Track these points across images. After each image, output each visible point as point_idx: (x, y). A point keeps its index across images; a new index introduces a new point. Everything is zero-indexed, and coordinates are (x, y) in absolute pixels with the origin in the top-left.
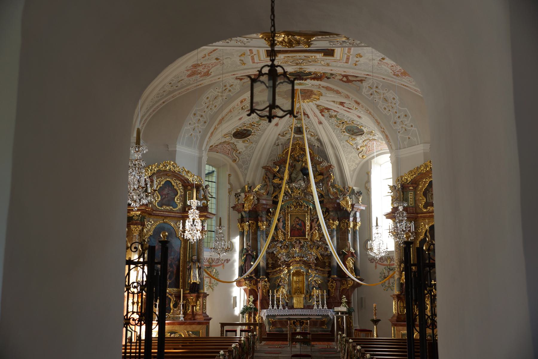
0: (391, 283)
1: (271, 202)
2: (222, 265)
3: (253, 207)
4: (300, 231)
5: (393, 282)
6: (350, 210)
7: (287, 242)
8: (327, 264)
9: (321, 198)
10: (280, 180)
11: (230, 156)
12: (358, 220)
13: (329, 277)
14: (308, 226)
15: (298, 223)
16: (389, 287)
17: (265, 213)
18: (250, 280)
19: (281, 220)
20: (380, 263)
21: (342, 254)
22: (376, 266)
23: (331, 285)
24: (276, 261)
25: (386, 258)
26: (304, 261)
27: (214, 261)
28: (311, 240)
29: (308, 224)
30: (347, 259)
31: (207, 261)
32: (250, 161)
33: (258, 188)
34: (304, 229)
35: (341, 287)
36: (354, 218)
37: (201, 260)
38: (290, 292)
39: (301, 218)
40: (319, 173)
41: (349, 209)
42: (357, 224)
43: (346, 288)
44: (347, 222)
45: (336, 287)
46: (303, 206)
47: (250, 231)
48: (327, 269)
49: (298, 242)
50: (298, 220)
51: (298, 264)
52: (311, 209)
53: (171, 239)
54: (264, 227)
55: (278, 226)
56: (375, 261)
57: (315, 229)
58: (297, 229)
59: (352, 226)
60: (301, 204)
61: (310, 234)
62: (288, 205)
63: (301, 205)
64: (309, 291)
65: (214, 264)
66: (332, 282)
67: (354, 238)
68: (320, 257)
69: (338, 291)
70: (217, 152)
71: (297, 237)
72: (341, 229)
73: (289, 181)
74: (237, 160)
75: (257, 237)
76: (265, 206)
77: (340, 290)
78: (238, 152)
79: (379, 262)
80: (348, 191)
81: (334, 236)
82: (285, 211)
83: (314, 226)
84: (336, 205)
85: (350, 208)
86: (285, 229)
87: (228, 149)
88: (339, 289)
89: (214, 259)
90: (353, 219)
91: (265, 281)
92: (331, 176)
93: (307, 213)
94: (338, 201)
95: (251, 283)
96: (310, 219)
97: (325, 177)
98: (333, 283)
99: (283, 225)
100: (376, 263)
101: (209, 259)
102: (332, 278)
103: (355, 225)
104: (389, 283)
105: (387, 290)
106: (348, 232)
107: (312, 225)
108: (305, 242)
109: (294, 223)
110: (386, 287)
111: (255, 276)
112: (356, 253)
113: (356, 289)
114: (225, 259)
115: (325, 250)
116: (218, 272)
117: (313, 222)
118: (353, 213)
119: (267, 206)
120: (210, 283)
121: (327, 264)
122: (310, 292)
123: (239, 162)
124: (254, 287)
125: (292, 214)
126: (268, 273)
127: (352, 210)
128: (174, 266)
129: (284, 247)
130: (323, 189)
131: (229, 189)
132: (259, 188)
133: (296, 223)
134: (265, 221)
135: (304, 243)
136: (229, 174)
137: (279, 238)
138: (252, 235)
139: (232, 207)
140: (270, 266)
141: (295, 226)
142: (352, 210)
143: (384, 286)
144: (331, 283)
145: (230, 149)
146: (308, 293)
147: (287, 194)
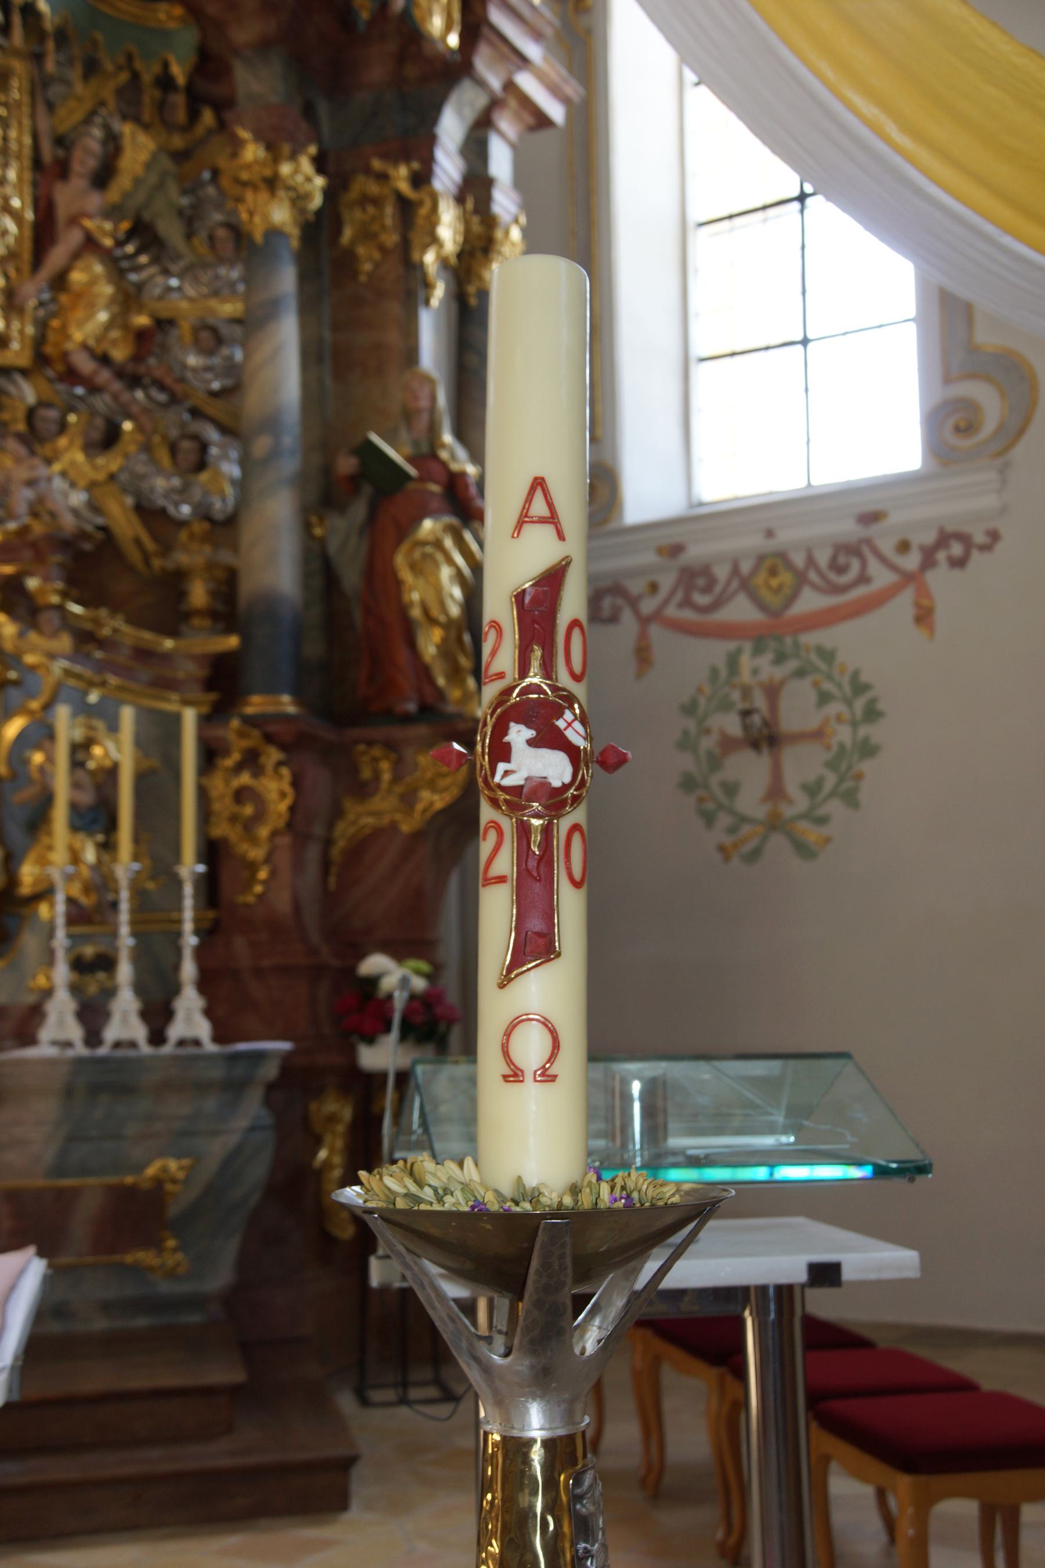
0: (792, 785)
5: (811, 778)
8: (198, 594)
16: (775, 824)
20: (688, 615)
21: (354, 482)
22: (643, 655)
23: (240, 795)
25: (746, 567)
28: (41, 359)
30: (406, 527)
35: (337, 813)
42: (499, 234)
43: (394, 826)
56: (633, 603)
69: (313, 854)
77: (328, 842)
79: (672, 611)
88: (318, 830)
98: (258, 771)
100: (644, 621)
104: (776, 792)
105: (754, 855)
110: (745, 829)
121: (198, 594)
143: (724, 820)
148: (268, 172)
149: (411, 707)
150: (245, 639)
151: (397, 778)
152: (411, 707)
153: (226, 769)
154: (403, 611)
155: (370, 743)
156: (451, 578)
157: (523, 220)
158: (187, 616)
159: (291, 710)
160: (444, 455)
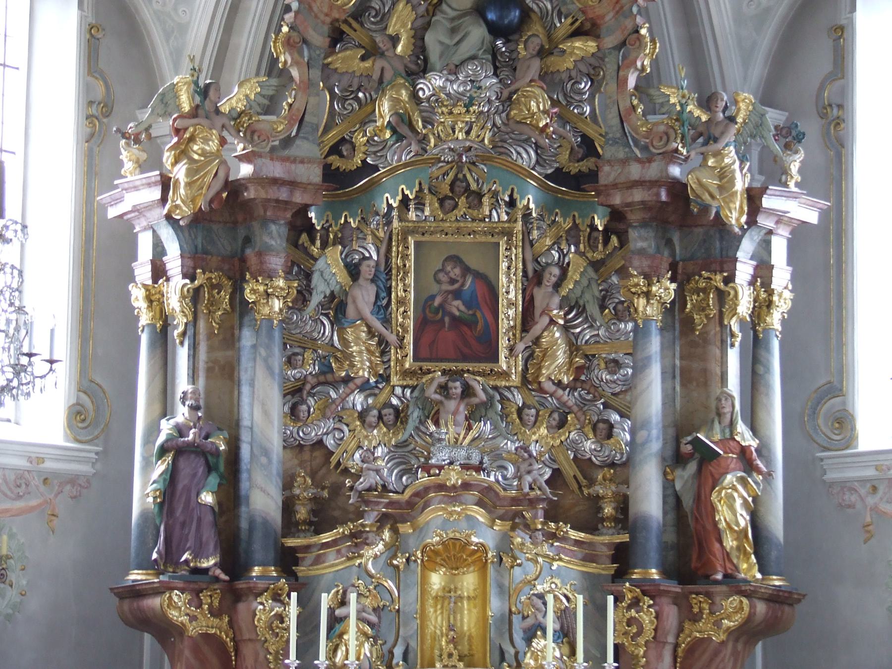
1: (315, 174)
3: (219, 193)
4: (465, 329)
6: (738, 220)
7: (398, 391)
8: (608, 510)
9: (582, 159)
10: (363, 58)
12: (781, 277)
13: (620, 575)
14: (511, 304)
15: (456, 286)
17: (284, 231)
18: (192, 586)
19: (367, 270)
24: (337, 490)
26: (488, 490)
29: (512, 295)
30: (716, 482)
33: (247, 96)
34: (490, 318)
36: (756, 268)
38: (411, 656)
39: (473, 262)
40: (577, 24)
41: (735, 216)
42: (775, 298)
43: (709, 639)
44: (721, 285)
45: (655, 630)
46: (486, 200)
47: (202, 324)
48: (608, 538)
49: (457, 387)
50: (457, 271)
51: (454, 500)
52: (527, 216)
54: (277, 304)
55: (350, 301)
57: (545, 320)
58: (454, 318)
59: (744, 307)
60: (474, 186)
61: (521, 346)
62: (407, 192)
63: (474, 192)
64: (512, 651)
66: (635, 603)
67: (754, 373)
68: (570, 471)
71: (449, 360)
72: (688, 324)
73: (413, 67)
75: (239, 360)
76: (283, 194)
77: (676, 646)
80: (732, 119)
81: (648, 360)
82: (389, 223)
83: (544, 306)
84: (668, 195)
85: (741, 212)
86: (387, 321)
88: (671, 639)
90: (751, 271)
91: (277, 598)
92: (640, 38)
93: (509, 234)
94: (675, 171)
95: (199, 606)
96: (525, 271)
97: (610, 41)
99: (377, 296)
102: (634, 583)
103: (762, 306)
106: (723, 342)
107: (532, 298)
108: (495, 388)
109: (434, 288)
111: (221, 565)
112: (764, 450)
113: (760, 645)
115: (598, 433)
117: (539, 283)
118: (752, 239)
119: (291, 192)
121: (608, 510)
122: (517, 653)
124: (216, 626)
125: (427, 238)
126: (294, 550)
127: (752, 222)
129: (380, 417)
130: (593, 110)
132: (252, 97)
133: (446, 287)
134: (281, 273)
135: (491, 398)
137: (352, 365)
138: (211, 349)
140: (302, 513)
141: (441, 306)
142: (752, 222)
144: (629, 607)
146: (503, 658)
147: (404, 130)
148: (645, 289)
149: (719, 577)
150: (632, 537)
151: (712, 613)
152: (719, 577)
153: (623, 607)
154: (715, 524)
155: (697, 594)
156: (742, 504)
157: (790, 287)
158: (603, 520)
159: (656, 577)
160: (738, 438)
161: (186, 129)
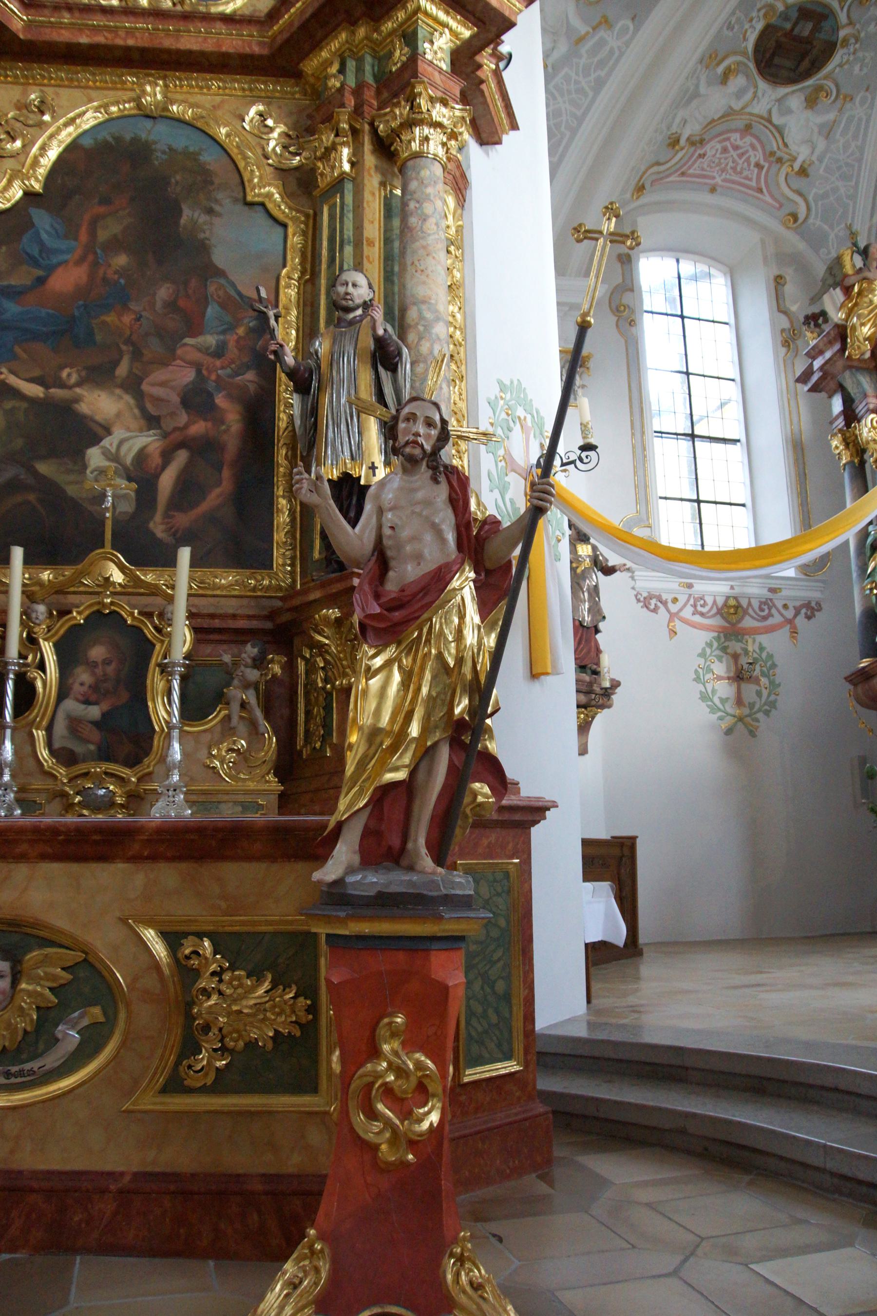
2: (788, 627)
11: (768, 198)
27: (750, 611)
31: (714, 610)
32: (853, 197)
37: (412, 314)
53: (203, 218)
65: (748, 623)
70: (713, 190)
74: (802, 216)
78: (797, 166)
87: (753, 160)
89: (750, 604)
101: (728, 598)
114: (798, 604)
116: (770, 656)
120: (739, 702)
123: (811, 221)
128: (220, 400)
131: (783, 331)
136: (778, 273)
139: (798, 380)
145: (762, 162)
161: (854, 285)
